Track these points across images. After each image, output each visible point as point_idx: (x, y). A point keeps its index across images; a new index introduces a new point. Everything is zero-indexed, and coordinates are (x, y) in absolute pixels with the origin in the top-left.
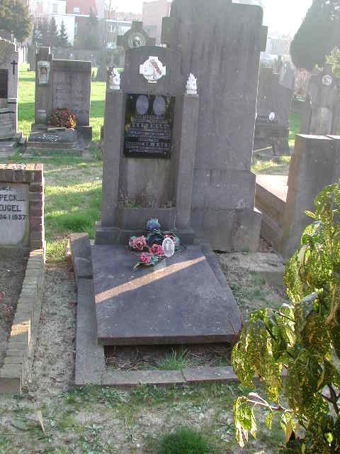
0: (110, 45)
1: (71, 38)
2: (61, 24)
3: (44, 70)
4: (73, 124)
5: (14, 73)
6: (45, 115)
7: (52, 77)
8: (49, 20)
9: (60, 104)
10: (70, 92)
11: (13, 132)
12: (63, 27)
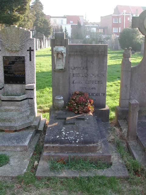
0: (87, 37)
1: (70, 35)
2: (65, 28)
3: (60, 56)
4: (91, 108)
5: (30, 60)
6: (63, 102)
7: (68, 62)
8: (59, 27)
9: (76, 88)
10: (86, 76)
11: (32, 118)
12: (66, 29)
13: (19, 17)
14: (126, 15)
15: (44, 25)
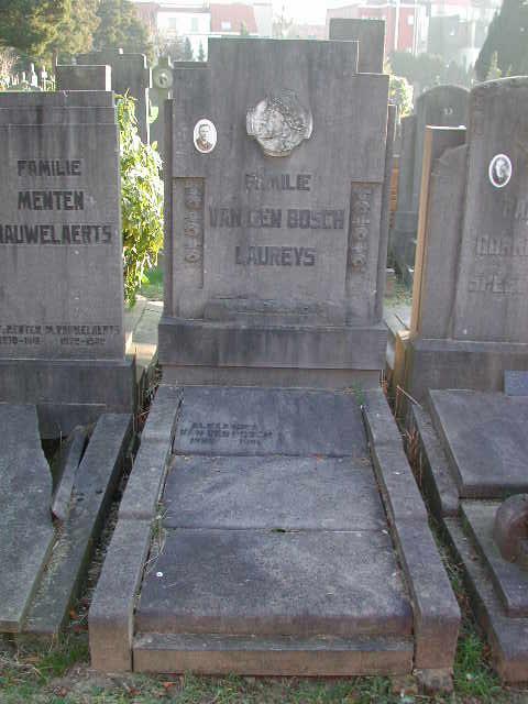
8: (183, 45)
13: (46, 30)
15: (129, 40)
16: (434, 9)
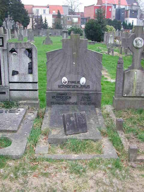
2: (45, 18)
12: (45, 19)
14: (107, 5)
16: (117, 7)
